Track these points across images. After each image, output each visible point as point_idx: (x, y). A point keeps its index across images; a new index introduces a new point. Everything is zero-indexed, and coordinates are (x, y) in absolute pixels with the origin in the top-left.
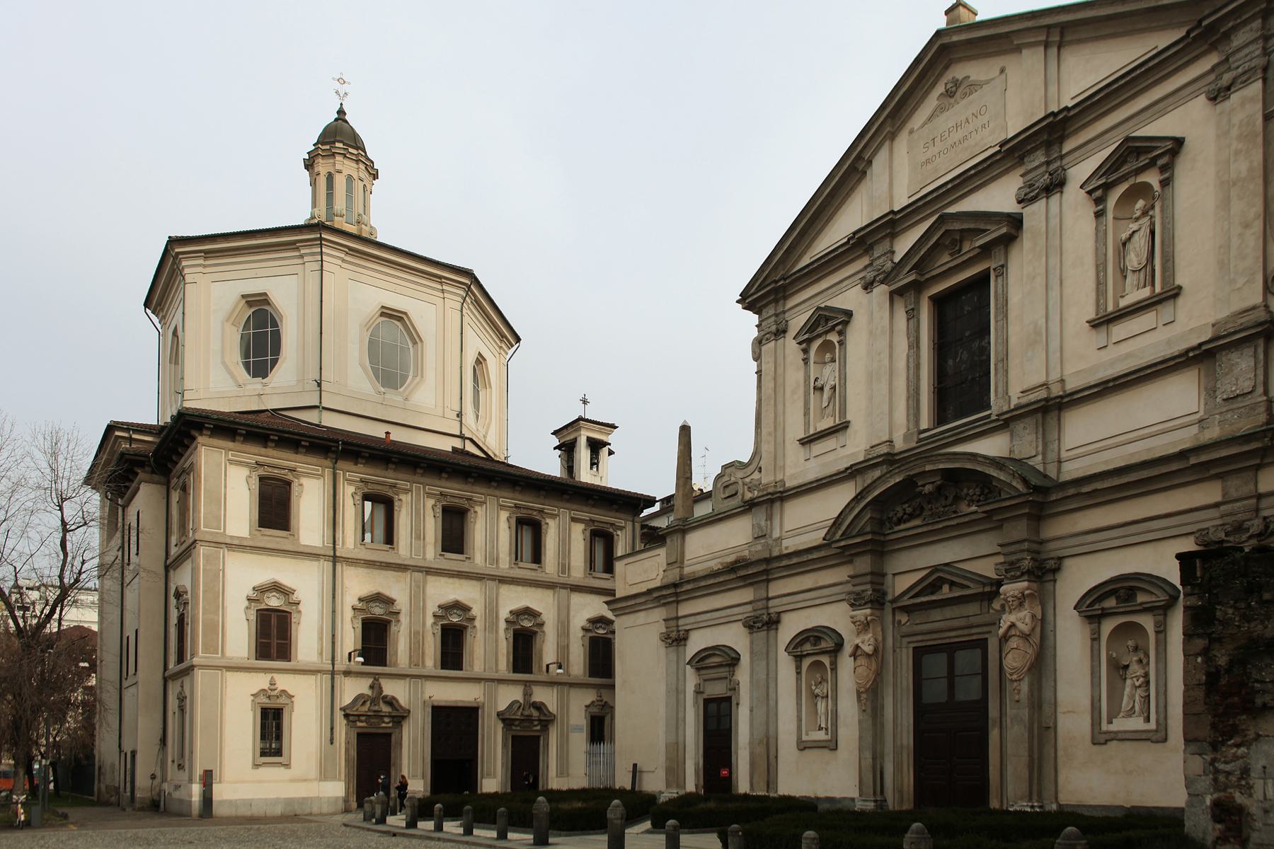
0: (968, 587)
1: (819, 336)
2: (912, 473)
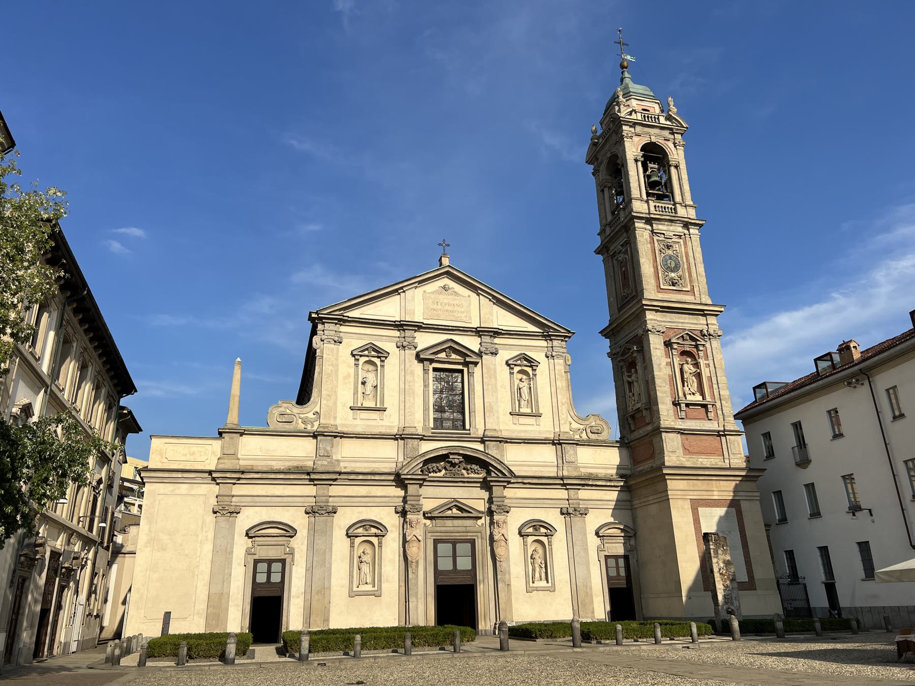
1: (367, 356)
2: (452, 452)
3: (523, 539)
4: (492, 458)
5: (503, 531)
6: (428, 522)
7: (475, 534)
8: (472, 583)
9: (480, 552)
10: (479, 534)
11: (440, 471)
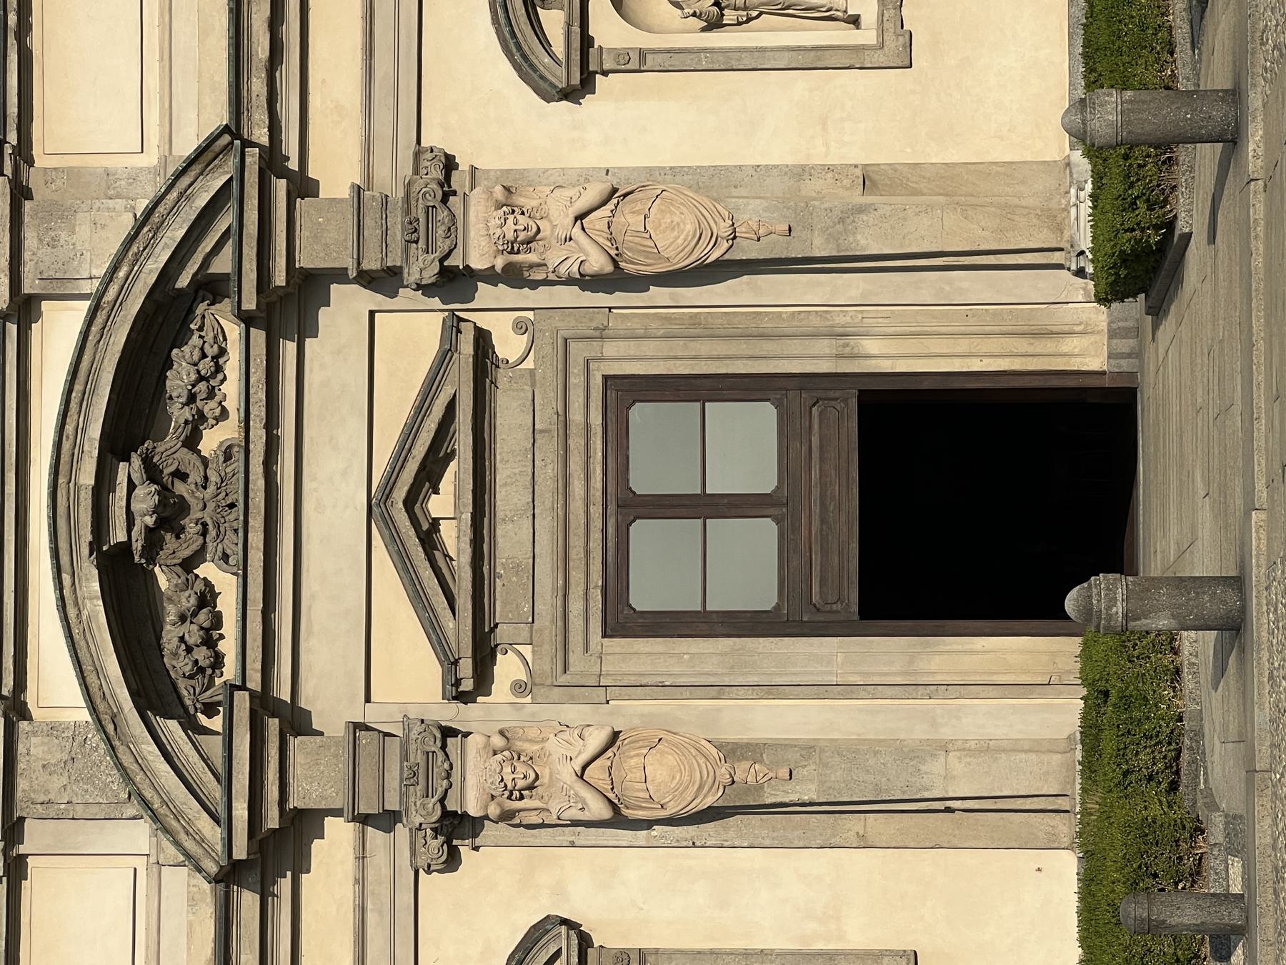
0: (451, 407)
2: (87, 536)
3: (605, 73)
4: (122, 274)
5: (559, 217)
6: (507, 669)
7: (576, 380)
8: (854, 403)
9: (678, 347)
10: (579, 351)
11: (207, 597)
